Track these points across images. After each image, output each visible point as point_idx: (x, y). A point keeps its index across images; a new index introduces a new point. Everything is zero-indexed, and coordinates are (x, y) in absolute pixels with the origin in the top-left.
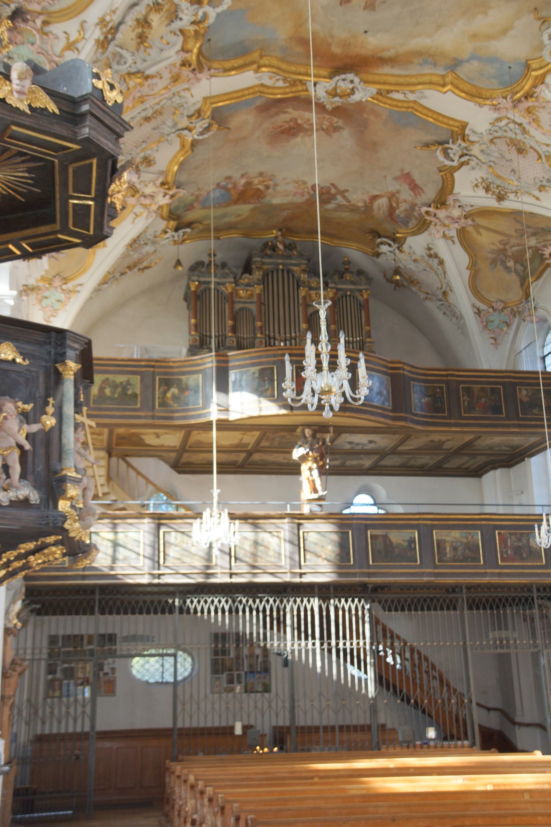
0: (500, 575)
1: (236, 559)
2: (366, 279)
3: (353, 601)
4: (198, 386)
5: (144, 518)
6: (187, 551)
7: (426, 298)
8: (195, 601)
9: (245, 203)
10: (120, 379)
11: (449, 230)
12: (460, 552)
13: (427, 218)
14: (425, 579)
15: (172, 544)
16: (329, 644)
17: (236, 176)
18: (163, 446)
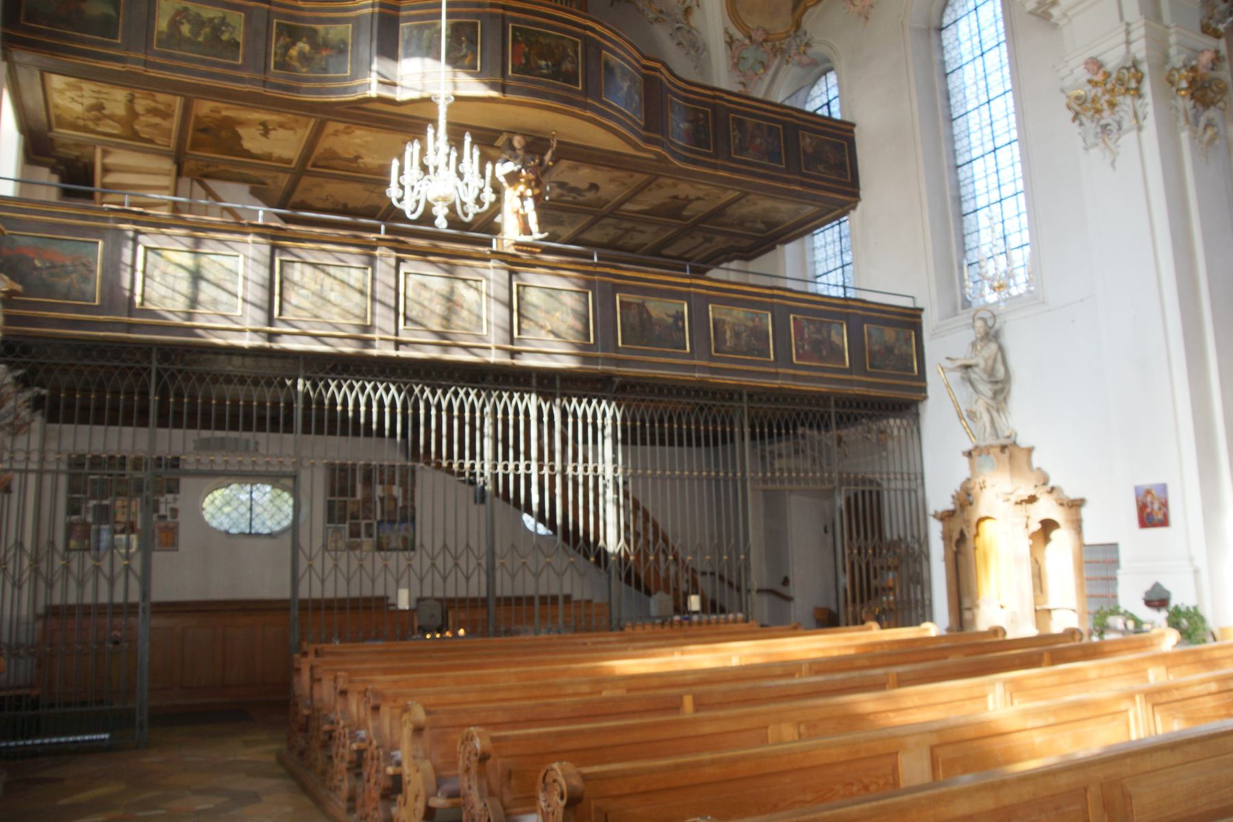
0: (795, 378)
1: (406, 318)
3: (589, 403)
4: (344, 42)
5: (247, 234)
6: (323, 298)
7: (656, 20)
8: (333, 385)
10: (210, 13)
12: (743, 342)
14: (697, 375)
15: (295, 284)
16: (552, 468)
18: (269, 157)
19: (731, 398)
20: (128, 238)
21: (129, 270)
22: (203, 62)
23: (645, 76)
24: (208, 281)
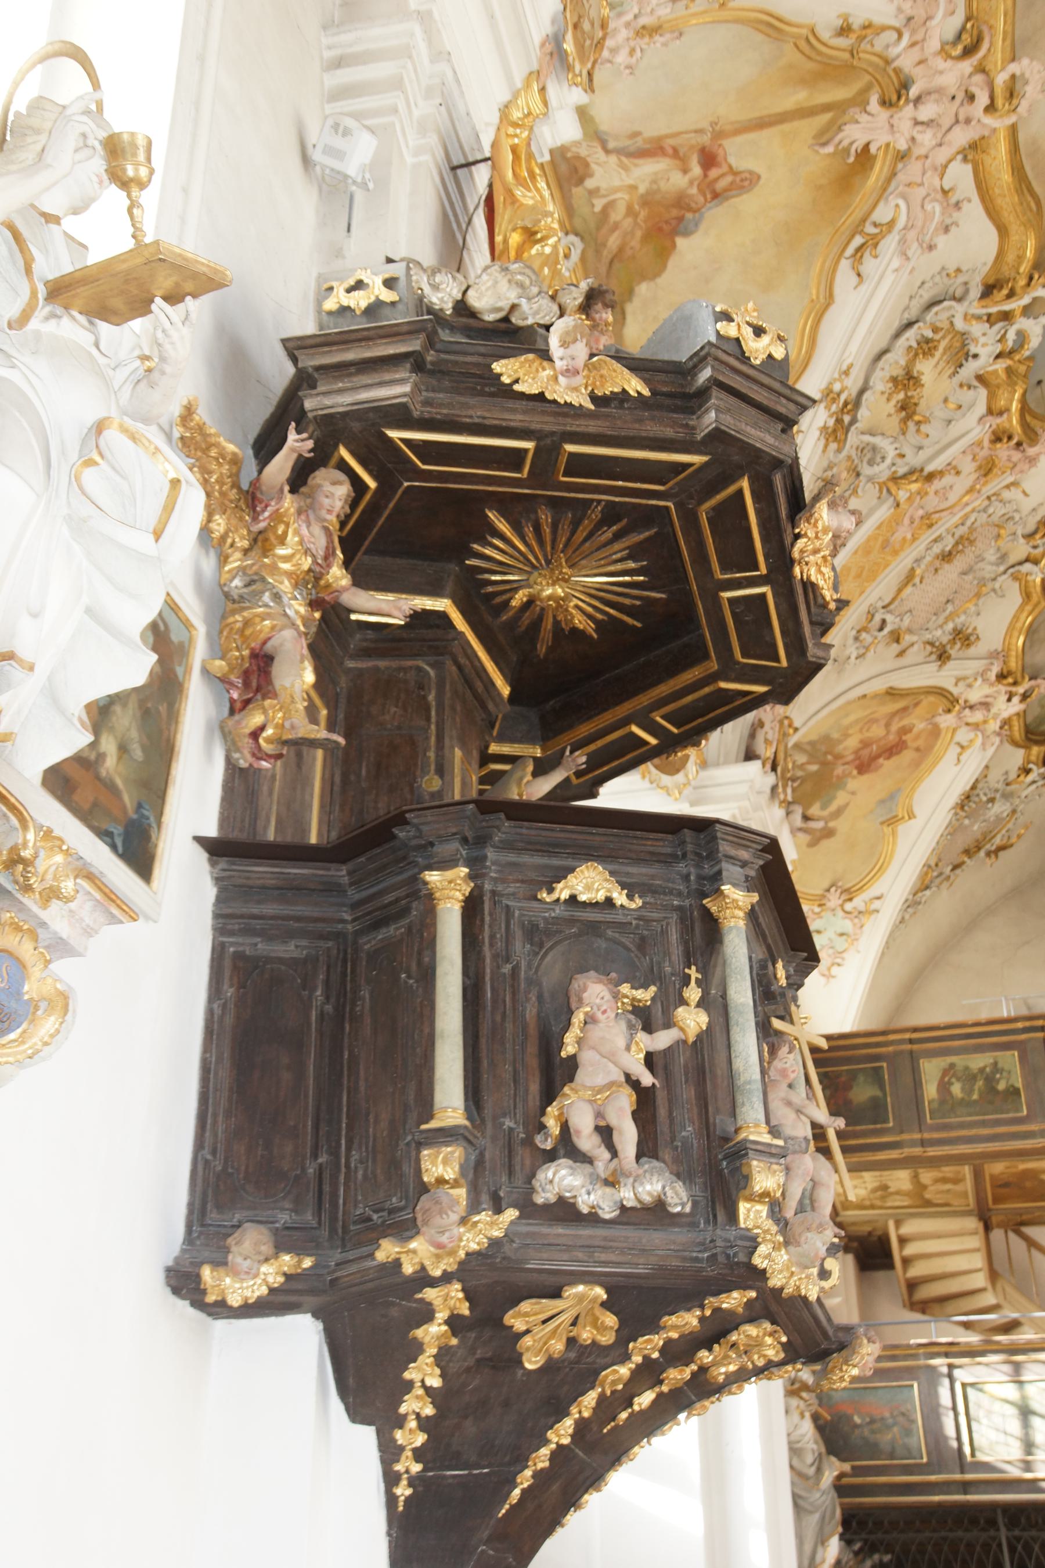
10: (979, 1061)
20: (941, 1375)
21: (951, 1414)
22: (983, 1124)
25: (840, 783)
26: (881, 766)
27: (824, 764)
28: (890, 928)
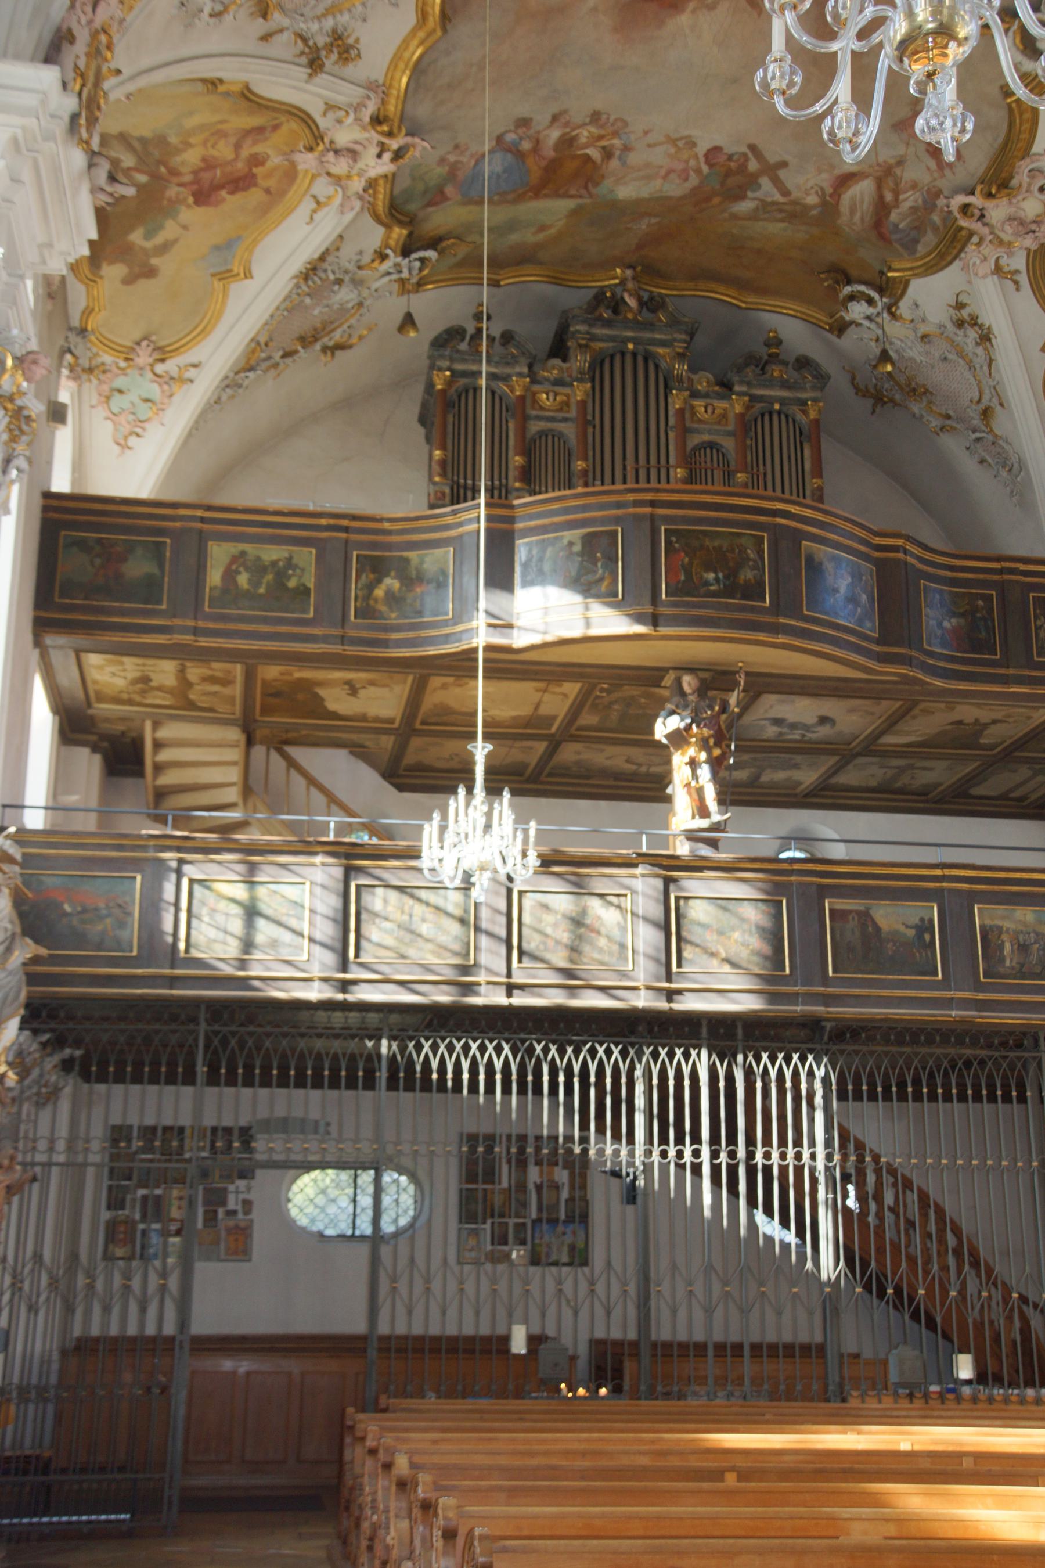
2: (815, 377)
4: (444, 573)
9: (557, 195)
10: (272, 553)
11: (1010, 254)
13: (963, 223)
17: (541, 119)
18: (363, 718)
19: (1019, 1046)
20: (170, 869)
21: (172, 909)
22: (265, 620)
23: (880, 564)
24: (267, 918)
25: (170, 210)
26: (224, 200)
27: (155, 176)
28: (199, 410)
